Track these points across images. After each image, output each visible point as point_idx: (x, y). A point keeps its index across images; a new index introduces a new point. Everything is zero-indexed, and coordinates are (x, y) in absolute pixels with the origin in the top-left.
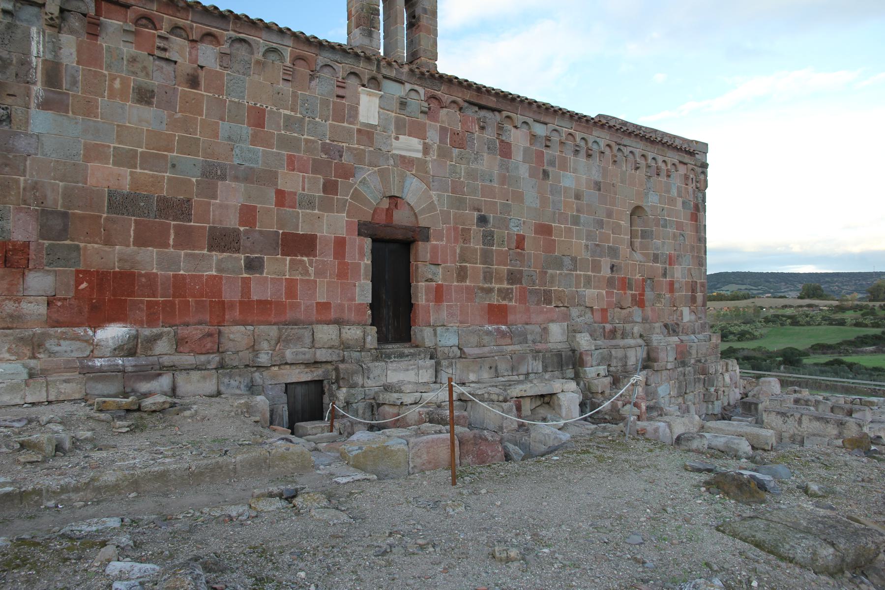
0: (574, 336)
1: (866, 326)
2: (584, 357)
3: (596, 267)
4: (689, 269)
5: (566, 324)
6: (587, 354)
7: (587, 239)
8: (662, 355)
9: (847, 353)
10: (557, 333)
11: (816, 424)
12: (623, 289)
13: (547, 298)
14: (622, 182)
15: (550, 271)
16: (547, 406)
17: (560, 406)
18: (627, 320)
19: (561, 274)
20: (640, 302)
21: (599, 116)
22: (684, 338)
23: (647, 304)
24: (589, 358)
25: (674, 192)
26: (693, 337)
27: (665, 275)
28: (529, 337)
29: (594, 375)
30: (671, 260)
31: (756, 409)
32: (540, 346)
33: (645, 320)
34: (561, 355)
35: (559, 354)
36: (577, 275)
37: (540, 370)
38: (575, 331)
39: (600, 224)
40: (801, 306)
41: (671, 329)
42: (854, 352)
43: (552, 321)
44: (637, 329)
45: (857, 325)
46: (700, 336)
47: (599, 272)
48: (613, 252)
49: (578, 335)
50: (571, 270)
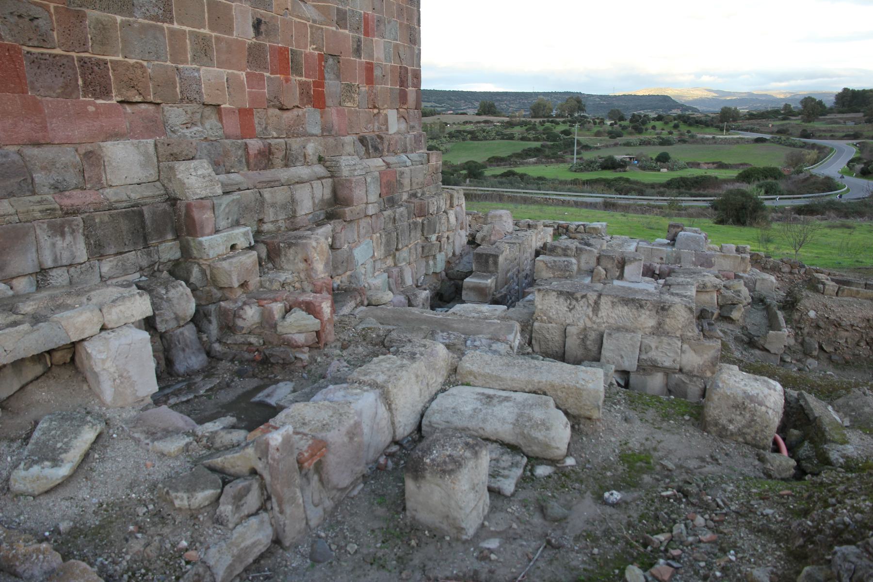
0: (172, 168)
1: (529, 140)
2: (196, 214)
4: (396, 47)
5: (151, 141)
6: (203, 207)
8: (358, 193)
9: (516, 165)
10: (127, 165)
11: (623, 311)
12: (284, 70)
13: (96, 79)
15: (93, 14)
16: (66, 373)
17: (96, 375)
18: (295, 131)
19: (127, 25)
22: (391, 159)
23: (329, 102)
24: (208, 215)
26: (404, 157)
27: (358, 51)
28: (39, 177)
29: (222, 249)
30: (367, 27)
31: (496, 263)
32: (76, 199)
33: (327, 131)
34: (141, 214)
35: (134, 213)
36: (172, 32)
37: (81, 253)
38: (175, 157)
40: (479, 122)
41: (372, 146)
42: (522, 164)
43: (116, 136)
44: (311, 148)
45: (523, 139)
46: (414, 156)
47: (230, 31)
49: (181, 167)
50: (156, 18)
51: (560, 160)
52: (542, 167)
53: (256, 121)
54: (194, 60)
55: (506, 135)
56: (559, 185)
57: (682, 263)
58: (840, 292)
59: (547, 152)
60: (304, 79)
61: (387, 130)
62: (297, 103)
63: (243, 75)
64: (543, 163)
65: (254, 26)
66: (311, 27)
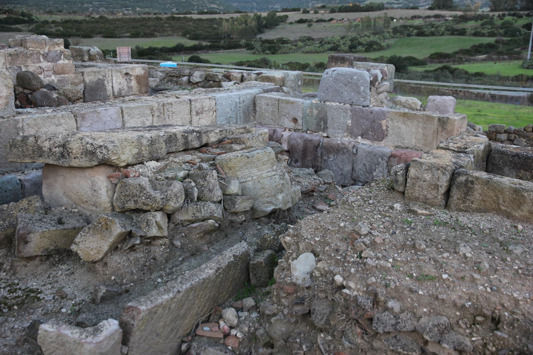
1: (483, 35)
9: (461, 61)
40: (429, 17)
42: (468, 61)
45: (476, 34)
51: (513, 56)
52: (492, 63)
55: (457, 30)
56: (501, 80)
57: (330, 131)
58: (456, 194)
59: (501, 48)
64: (493, 60)
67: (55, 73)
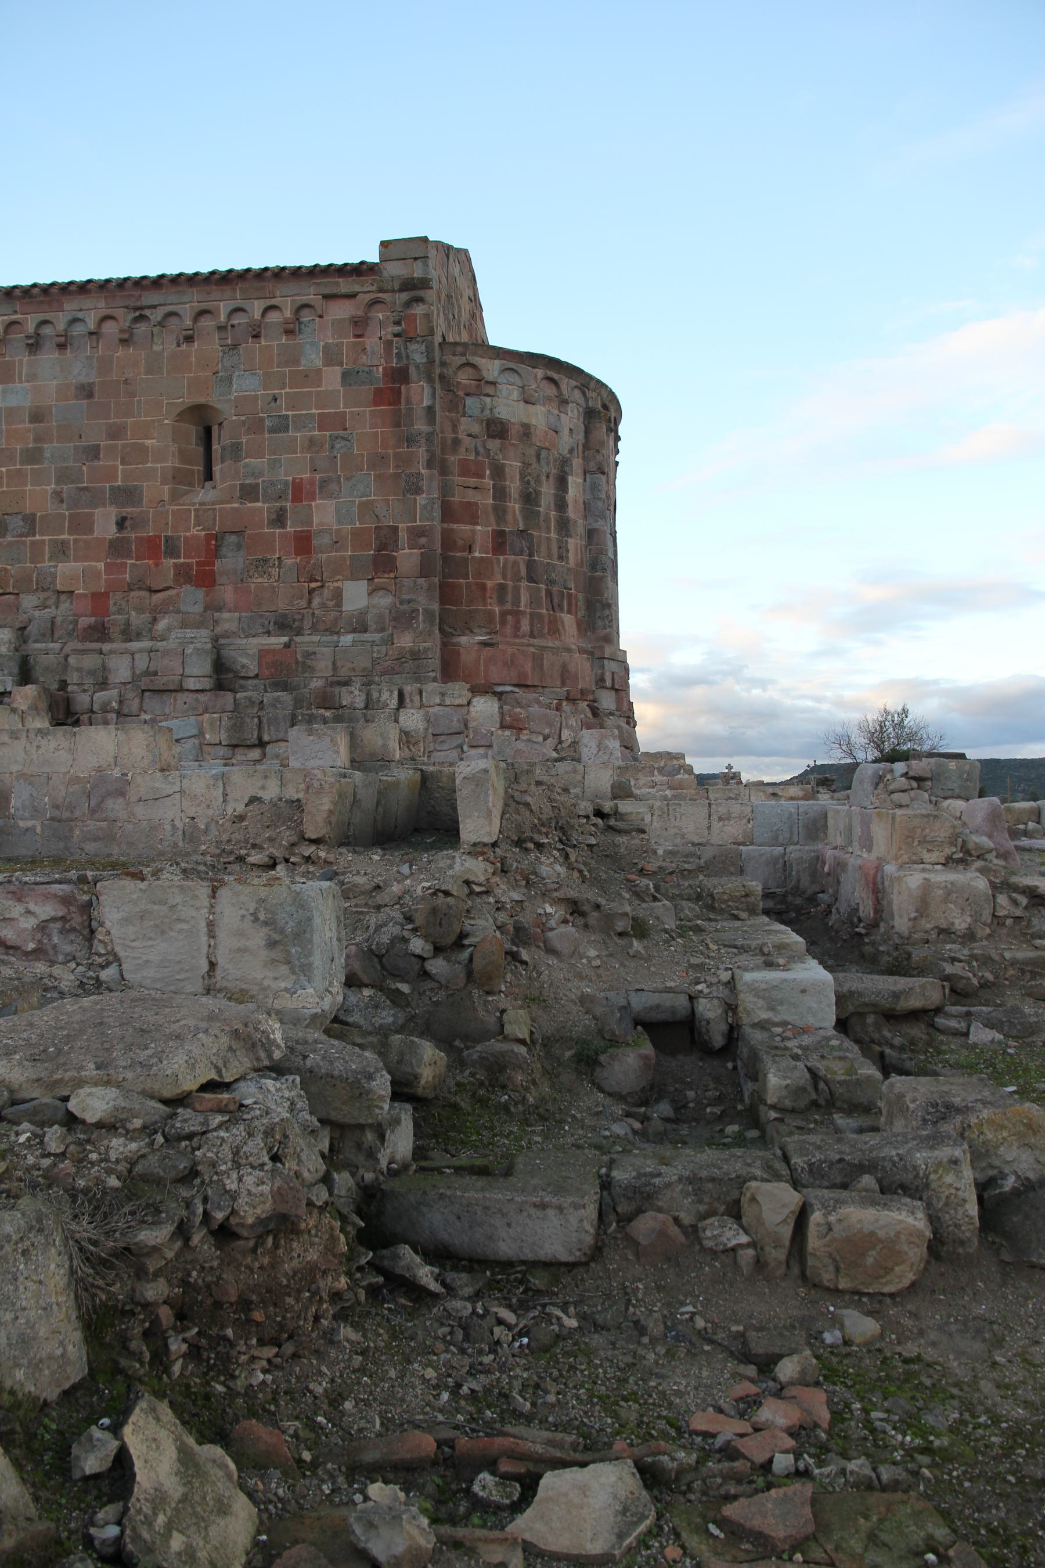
3: (81, 524)
7: (57, 483)
14: (149, 372)
20: (204, 578)
21: (362, 263)
23: (220, 579)
25: (313, 358)
36: (32, 543)
39: (93, 452)
47: (91, 531)
48: (126, 495)
50: (21, 535)
53: (111, 602)
54: (50, 559)
60: (182, 560)
61: (339, 604)
62: (170, 583)
63: (101, 566)
65: (117, 524)
66: (196, 510)
67: (670, 788)
